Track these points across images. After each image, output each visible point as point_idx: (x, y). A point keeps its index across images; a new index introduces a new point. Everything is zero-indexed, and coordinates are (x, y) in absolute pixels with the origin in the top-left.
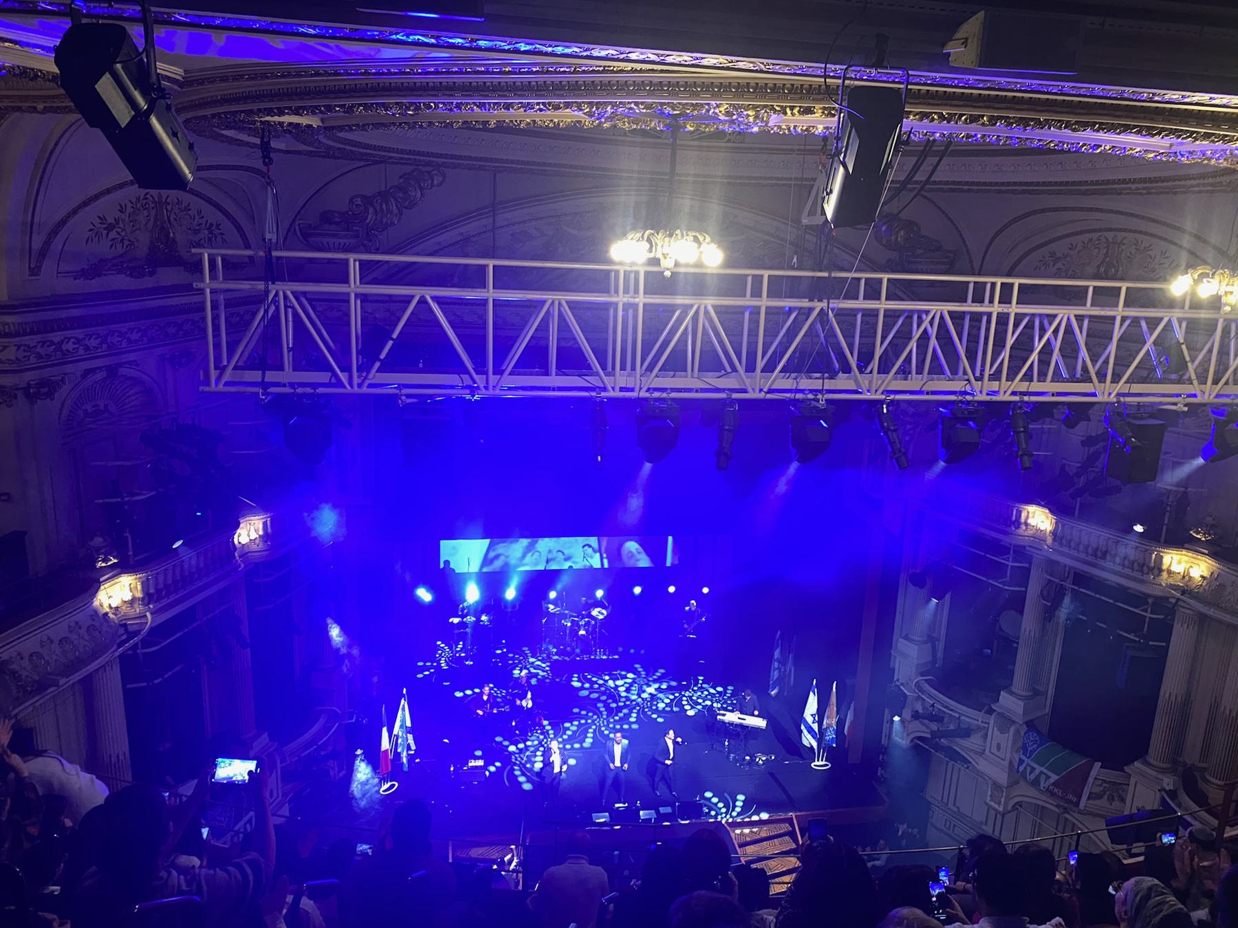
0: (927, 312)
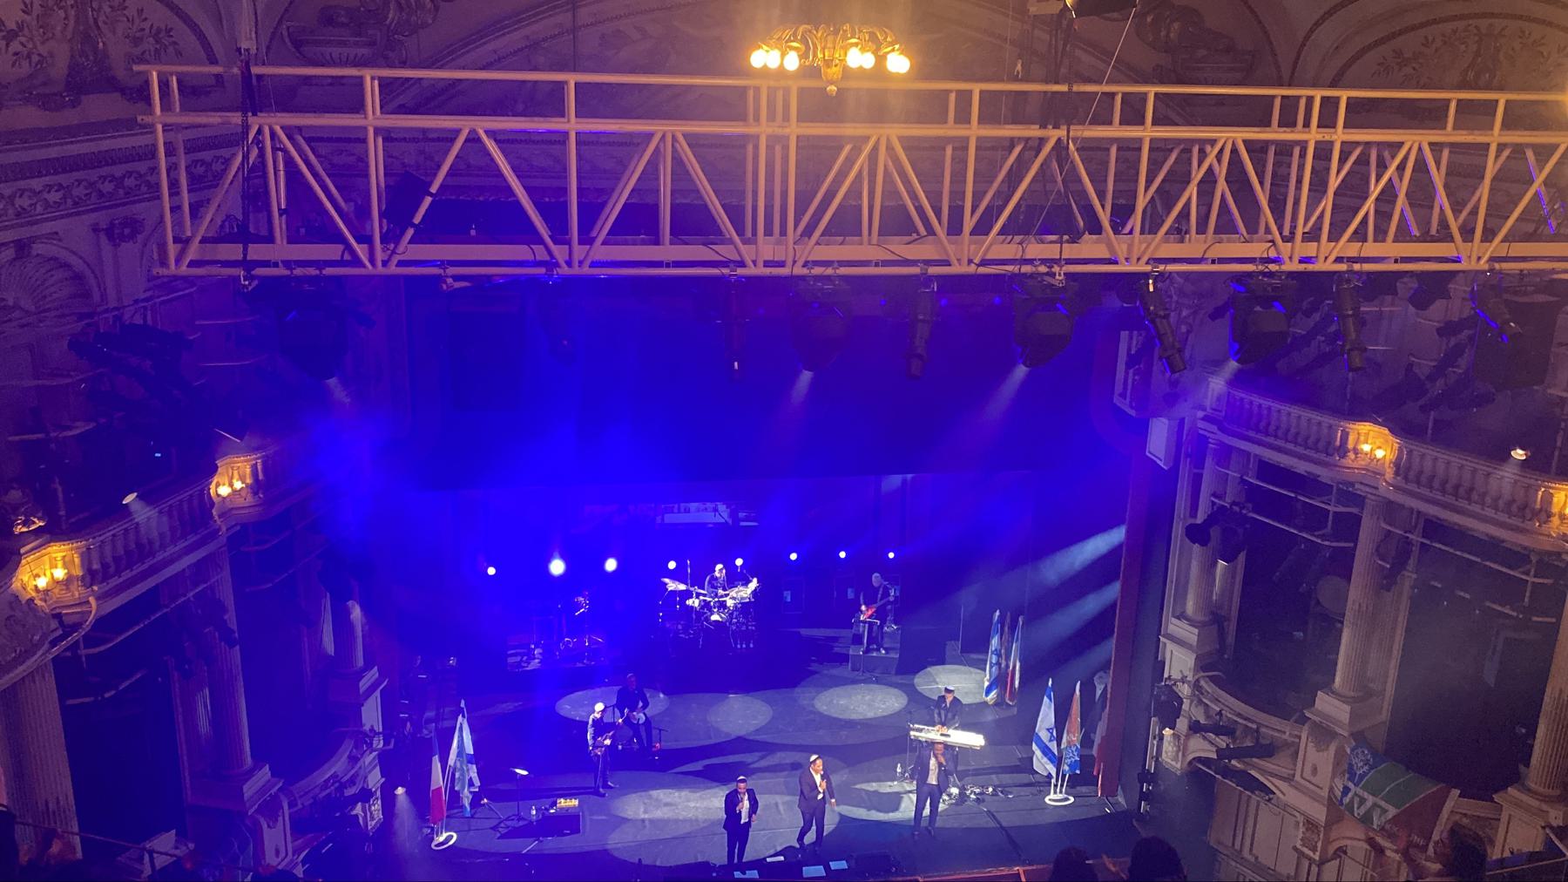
0: (1213, 142)
